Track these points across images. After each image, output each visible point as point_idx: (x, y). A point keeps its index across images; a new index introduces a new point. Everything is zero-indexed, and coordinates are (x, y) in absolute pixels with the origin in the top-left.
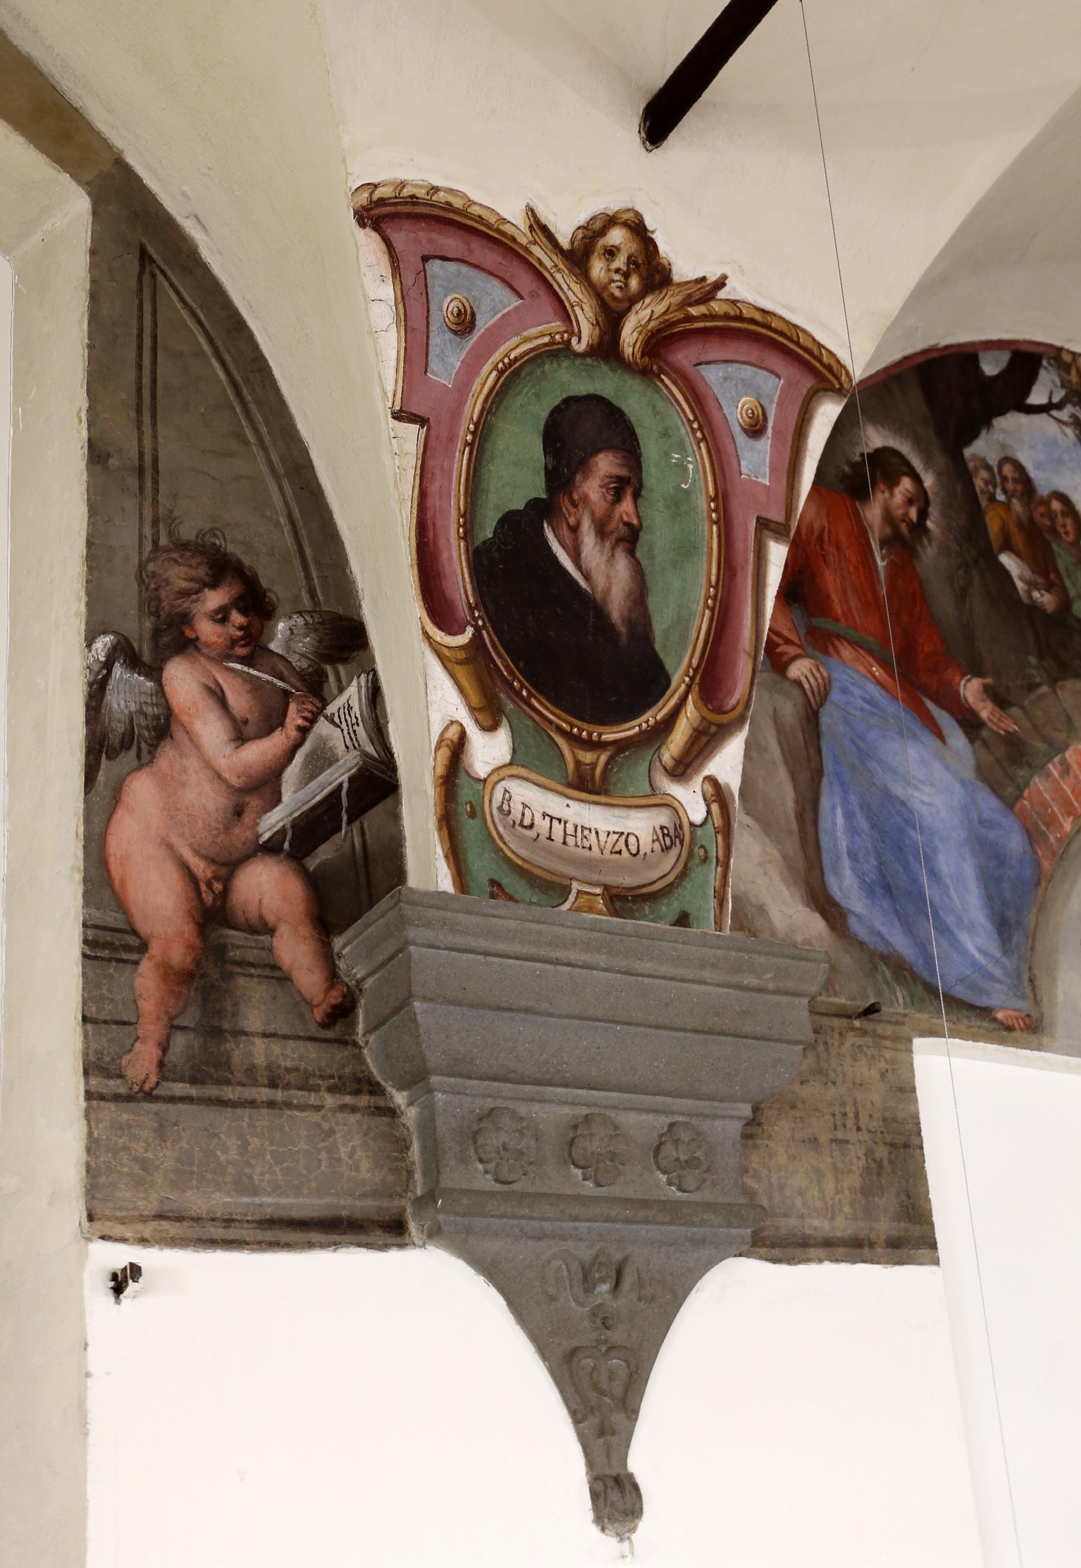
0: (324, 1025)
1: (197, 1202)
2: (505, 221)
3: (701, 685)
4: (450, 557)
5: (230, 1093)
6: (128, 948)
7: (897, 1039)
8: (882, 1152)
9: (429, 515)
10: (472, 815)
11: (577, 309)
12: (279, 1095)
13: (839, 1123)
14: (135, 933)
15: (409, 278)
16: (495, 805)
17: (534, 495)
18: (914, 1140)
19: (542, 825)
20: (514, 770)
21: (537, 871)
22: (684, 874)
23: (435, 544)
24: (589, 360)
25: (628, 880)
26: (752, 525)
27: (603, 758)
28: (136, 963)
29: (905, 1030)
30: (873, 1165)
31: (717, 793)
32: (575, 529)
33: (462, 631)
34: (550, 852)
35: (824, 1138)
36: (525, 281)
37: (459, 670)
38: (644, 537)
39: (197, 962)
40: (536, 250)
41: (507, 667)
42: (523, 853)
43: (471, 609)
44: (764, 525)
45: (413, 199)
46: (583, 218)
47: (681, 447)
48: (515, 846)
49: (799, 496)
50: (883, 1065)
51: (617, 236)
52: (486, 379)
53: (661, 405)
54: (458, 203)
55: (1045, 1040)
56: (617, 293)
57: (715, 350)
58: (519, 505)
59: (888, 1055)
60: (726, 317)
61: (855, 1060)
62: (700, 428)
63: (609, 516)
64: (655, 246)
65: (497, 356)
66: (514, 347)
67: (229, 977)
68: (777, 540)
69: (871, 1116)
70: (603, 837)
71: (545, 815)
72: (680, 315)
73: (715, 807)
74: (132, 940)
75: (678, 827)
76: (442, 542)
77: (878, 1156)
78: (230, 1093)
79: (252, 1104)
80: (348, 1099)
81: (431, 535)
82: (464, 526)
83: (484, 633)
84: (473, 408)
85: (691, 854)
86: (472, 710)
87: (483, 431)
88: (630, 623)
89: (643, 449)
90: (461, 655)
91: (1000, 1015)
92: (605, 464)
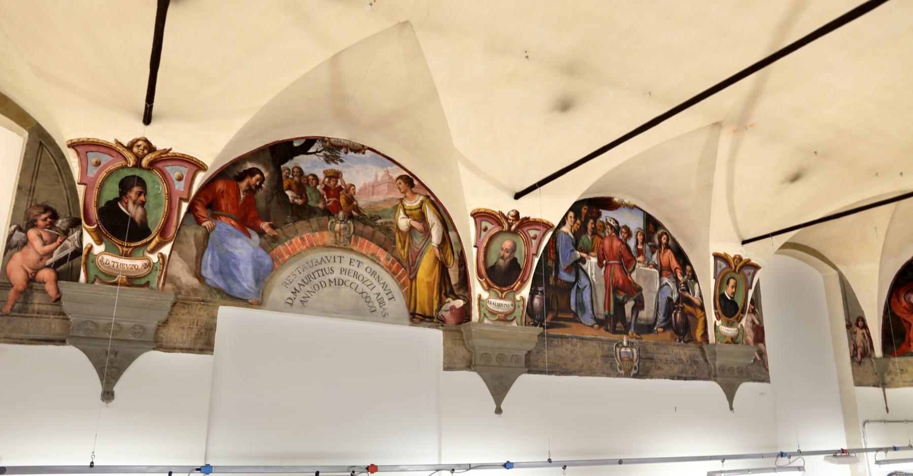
0: (54, 302)
1: (14, 335)
2: (109, 143)
3: (160, 234)
4: (92, 211)
5: (27, 315)
6: (8, 287)
7: (214, 306)
8: (203, 331)
9: (87, 203)
10: (92, 262)
11: (130, 159)
12: (39, 315)
13: (192, 323)
14: (11, 284)
15: (82, 157)
16: (99, 260)
17: (116, 197)
18: (214, 328)
19: (111, 264)
20: (105, 253)
21: (108, 273)
22: (150, 273)
23: (88, 208)
24: (132, 168)
25: (134, 274)
26: (178, 199)
27: (130, 249)
28: (10, 290)
29: (217, 305)
30: (199, 333)
31: (162, 256)
32: (127, 203)
33: (94, 225)
34: (113, 269)
35: (186, 327)
36: (115, 154)
37: (93, 234)
38: (146, 203)
39: (25, 290)
40: (118, 148)
41: (106, 232)
42: (105, 269)
43: (97, 221)
44: (181, 199)
45: (83, 141)
46: (130, 139)
47: (158, 184)
48: (103, 268)
49: (192, 193)
50: (208, 312)
51: (140, 143)
52: (104, 174)
53: (153, 176)
54: (95, 141)
55: (262, 307)
56: (141, 154)
57: (169, 163)
58: (111, 199)
59: (210, 310)
60: (172, 156)
61: (200, 310)
62: (164, 180)
63: (136, 200)
64: (151, 144)
65: (106, 170)
66: (111, 167)
67: (32, 292)
68: (185, 202)
69: (202, 323)
70: (128, 266)
71: (112, 262)
72: (159, 157)
73: (161, 259)
74: (10, 285)
75: (150, 264)
76: (90, 208)
77: (201, 331)
78: (27, 315)
79: (32, 317)
80: (57, 316)
81: (87, 207)
82: (96, 204)
83: (100, 226)
84: (99, 180)
85: (152, 269)
86: (95, 241)
87: (102, 185)
88: (141, 222)
89: (147, 185)
90: (93, 230)
91: (250, 301)
92: (136, 189)
